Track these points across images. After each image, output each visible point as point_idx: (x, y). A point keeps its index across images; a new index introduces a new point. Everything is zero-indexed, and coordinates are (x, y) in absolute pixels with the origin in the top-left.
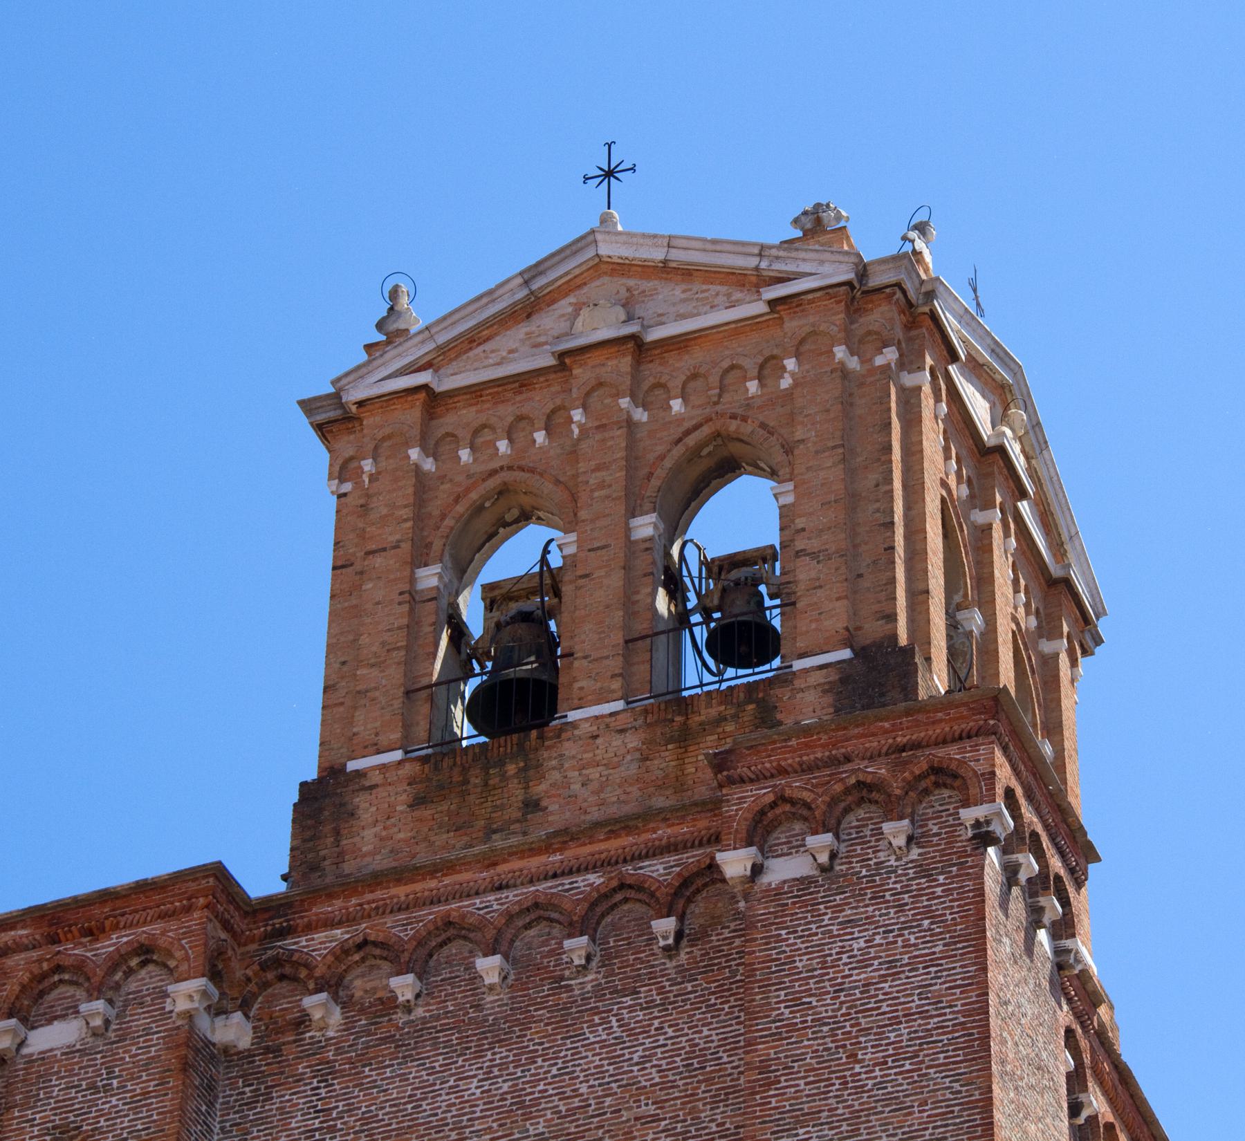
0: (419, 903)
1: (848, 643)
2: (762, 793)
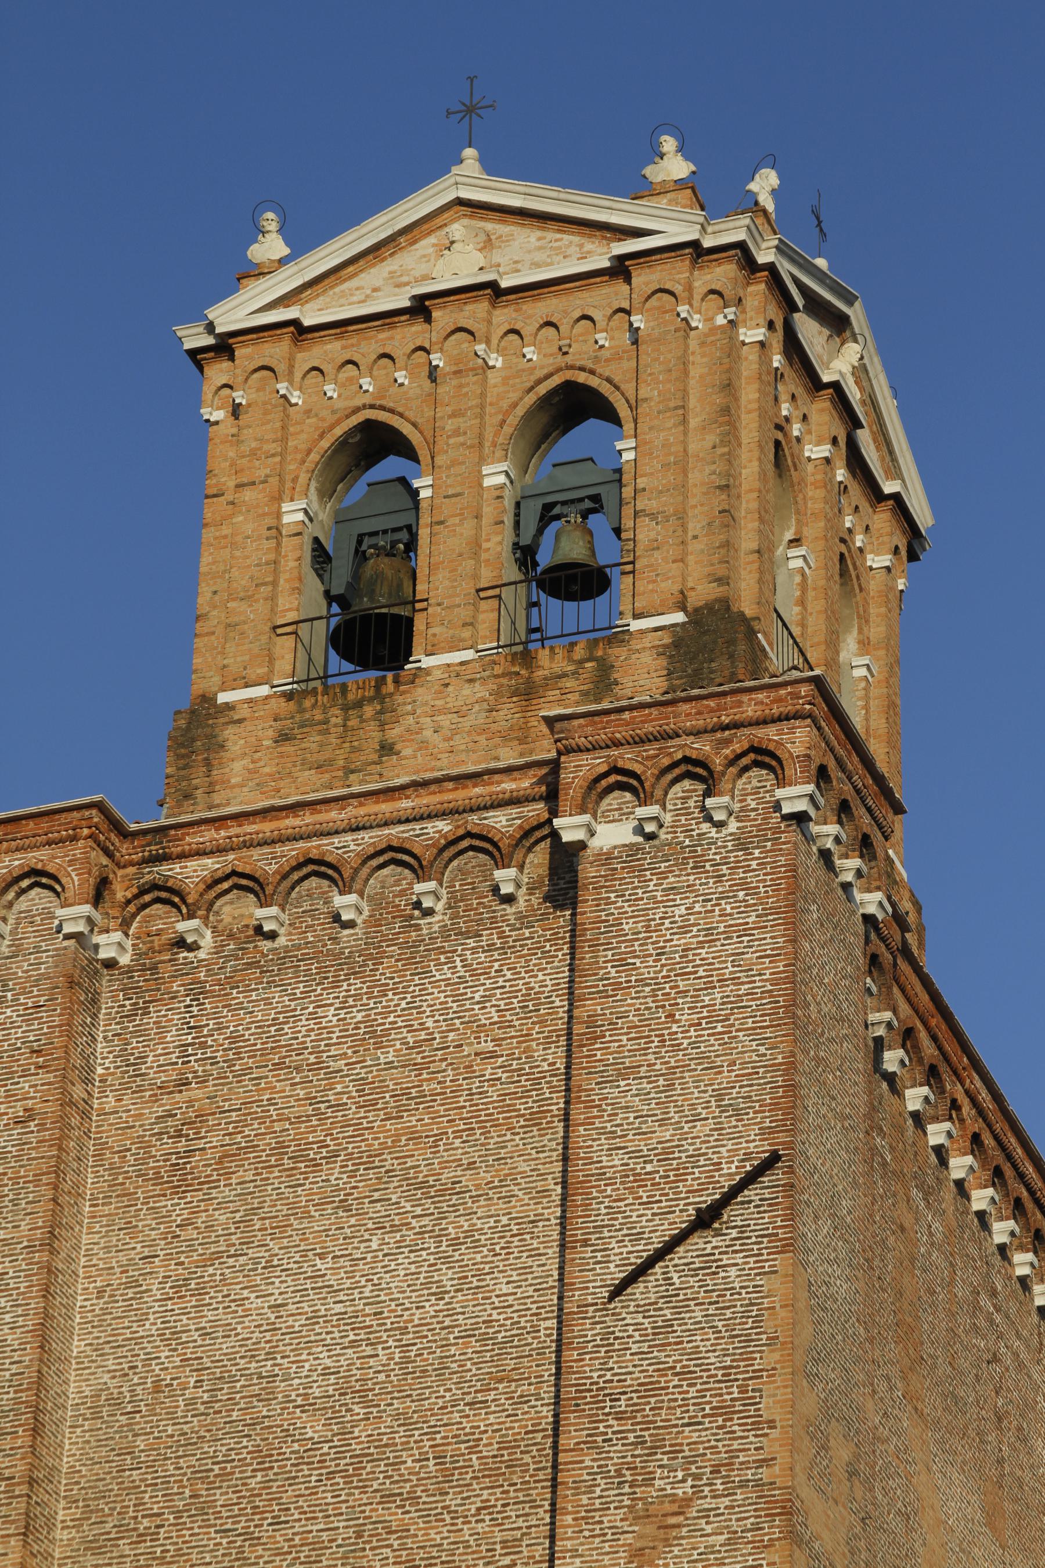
0: (281, 840)
1: (683, 607)
2: (597, 763)
